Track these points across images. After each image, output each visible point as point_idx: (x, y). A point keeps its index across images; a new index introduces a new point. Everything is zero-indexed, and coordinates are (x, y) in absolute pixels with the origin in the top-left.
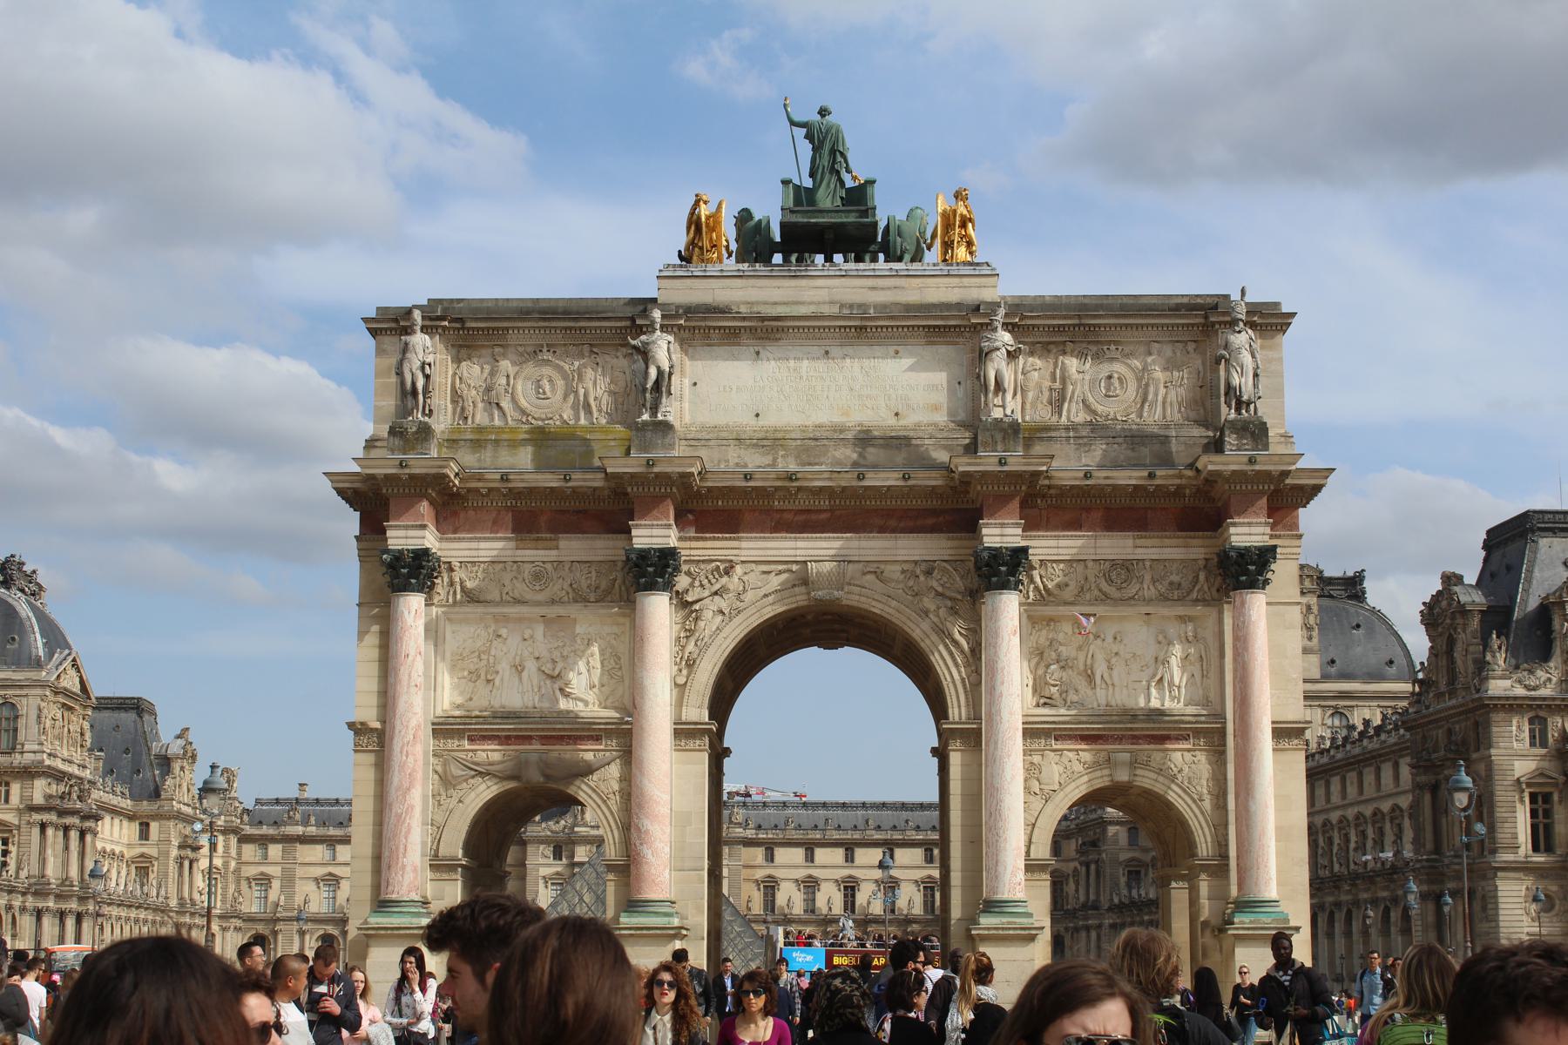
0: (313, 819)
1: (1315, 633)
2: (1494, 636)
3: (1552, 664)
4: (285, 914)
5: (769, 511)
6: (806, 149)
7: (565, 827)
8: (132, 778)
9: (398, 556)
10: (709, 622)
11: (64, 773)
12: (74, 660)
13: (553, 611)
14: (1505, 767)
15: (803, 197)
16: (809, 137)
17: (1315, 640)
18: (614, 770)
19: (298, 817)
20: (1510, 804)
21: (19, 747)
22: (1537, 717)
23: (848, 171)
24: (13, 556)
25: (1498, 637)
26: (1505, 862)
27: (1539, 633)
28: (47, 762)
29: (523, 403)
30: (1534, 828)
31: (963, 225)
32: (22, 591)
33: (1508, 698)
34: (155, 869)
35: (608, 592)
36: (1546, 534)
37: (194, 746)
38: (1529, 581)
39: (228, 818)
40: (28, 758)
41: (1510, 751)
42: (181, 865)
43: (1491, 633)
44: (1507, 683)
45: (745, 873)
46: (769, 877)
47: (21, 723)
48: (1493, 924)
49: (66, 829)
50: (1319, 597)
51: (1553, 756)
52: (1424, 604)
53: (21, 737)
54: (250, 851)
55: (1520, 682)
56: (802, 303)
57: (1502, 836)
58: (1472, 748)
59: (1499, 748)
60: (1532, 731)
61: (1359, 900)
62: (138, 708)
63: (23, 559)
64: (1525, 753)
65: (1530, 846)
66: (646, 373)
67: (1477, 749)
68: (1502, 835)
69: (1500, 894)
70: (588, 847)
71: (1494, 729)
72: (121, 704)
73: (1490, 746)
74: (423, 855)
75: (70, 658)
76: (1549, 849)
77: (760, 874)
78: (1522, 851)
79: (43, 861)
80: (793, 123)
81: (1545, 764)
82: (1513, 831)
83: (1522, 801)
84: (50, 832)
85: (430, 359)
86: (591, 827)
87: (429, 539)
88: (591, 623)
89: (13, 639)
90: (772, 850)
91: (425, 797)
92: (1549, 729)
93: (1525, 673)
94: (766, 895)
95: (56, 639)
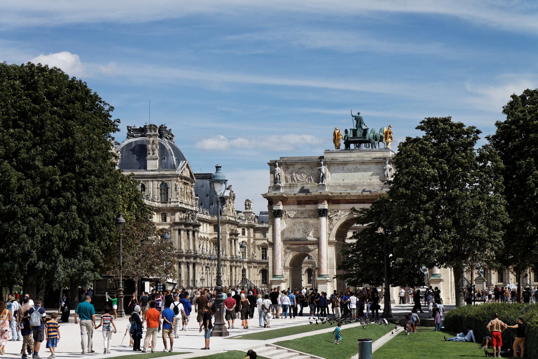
5: (345, 200)
6: (355, 122)
8: (210, 207)
9: (275, 211)
10: (334, 222)
11: (186, 209)
12: (187, 165)
13: (305, 220)
15: (354, 132)
16: (355, 119)
18: (317, 250)
21: (169, 200)
23: (364, 125)
24: (162, 125)
28: (180, 206)
29: (299, 179)
31: (390, 134)
32: (166, 138)
35: (315, 216)
37: (234, 192)
39: (249, 221)
40: (172, 205)
42: (231, 243)
47: (169, 190)
49: (188, 231)
53: (169, 197)
56: (352, 157)
63: (166, 126)
66: (320, 175)
74: (282, 266)
75: (186, 164)
79: (180, 243)
80: (353, 116)
84: (182, 232)
85: (280, 172)
87: (281, 207)
88: (312, 221)
89: (165, 158)
91: (282, 256)
95: (180, 157)
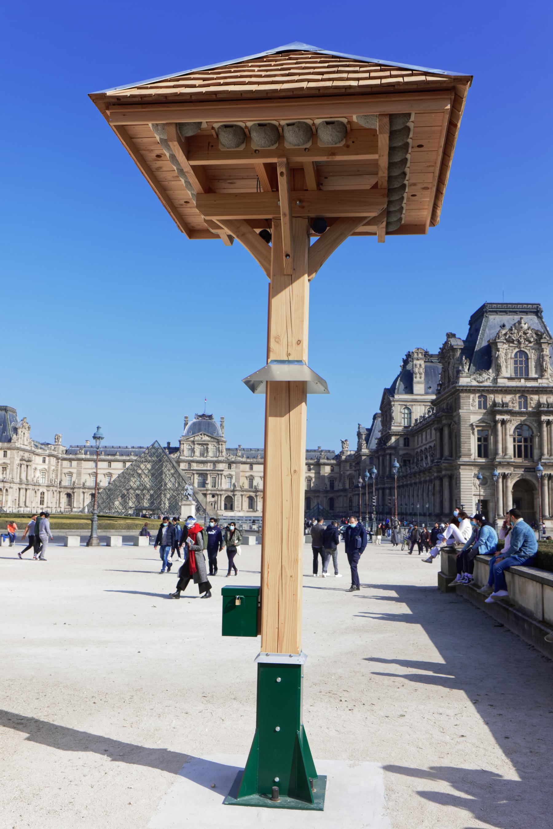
0: (88, 453)
1: (423, 376)
2: (464, 358)
3: (491, 371)
4: (77, 486)
14: (466, 418)
17: (423, 379)
19: (83, 452)
20: (468, 435)
22: (482, 395)
25: (466, 359)
26: (464, 462)
27: (486, 358)
30: (479, 447)
33: (467, 386)
34: (9, 468)
36: (493, 313)
38: (483, 334)
39: (50, 451)
41: (469, 411)
43: (463, 357)
44: (468, 380)
45: (241, 474)
46: (251, 475)
48: (458, 490)
50: (425, 362)
51: (489, 413)
52: (440, 348)
54: (66, 463)
55: (475, 379)
57: (464, 450)
58: (454, 411)
59: (463, 409)
60: (480, 402)
61: (421, 482)
64: (476, 412)
65: (477, 454)
67: (455, 411)
68: (464, 450)
69: (461, 476)
70: (185, 464)
71: (462, 401)
73: (460, 408)
76: (486, 456)
77: (248, 474)
78: (473, 457)
81: (486, 417)
82: (468, 447)
83: (473, 433)
86: (186, 457)
90: (230, 465)
92: (488, 401)
93: (478, 376)
94: (250, 482)
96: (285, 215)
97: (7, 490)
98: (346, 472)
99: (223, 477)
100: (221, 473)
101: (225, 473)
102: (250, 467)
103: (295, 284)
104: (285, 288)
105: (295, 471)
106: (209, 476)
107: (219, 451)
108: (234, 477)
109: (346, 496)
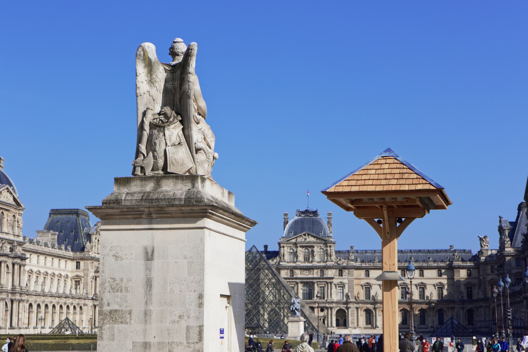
7: (276, 262)
34: (83, 281)
45: (356, 282)
46: (367, 283)
62: (77, 213)
70: (286, 271)
72: (70, 212)
77: (363, 282)
86: (288, 262)
90: (342, 271)
96: (387, 221)
97: (81, 308)
98: (486, 276)
99: (333, 286)
100: (331, 281)
101: (335, 281)
102: (366, 273)
103: (392, 242)
104: (388, 244)
105: (394, 312)
106: (316, 285)
107: (327, 254)
108: (347, 286)
109: (488, 307)
